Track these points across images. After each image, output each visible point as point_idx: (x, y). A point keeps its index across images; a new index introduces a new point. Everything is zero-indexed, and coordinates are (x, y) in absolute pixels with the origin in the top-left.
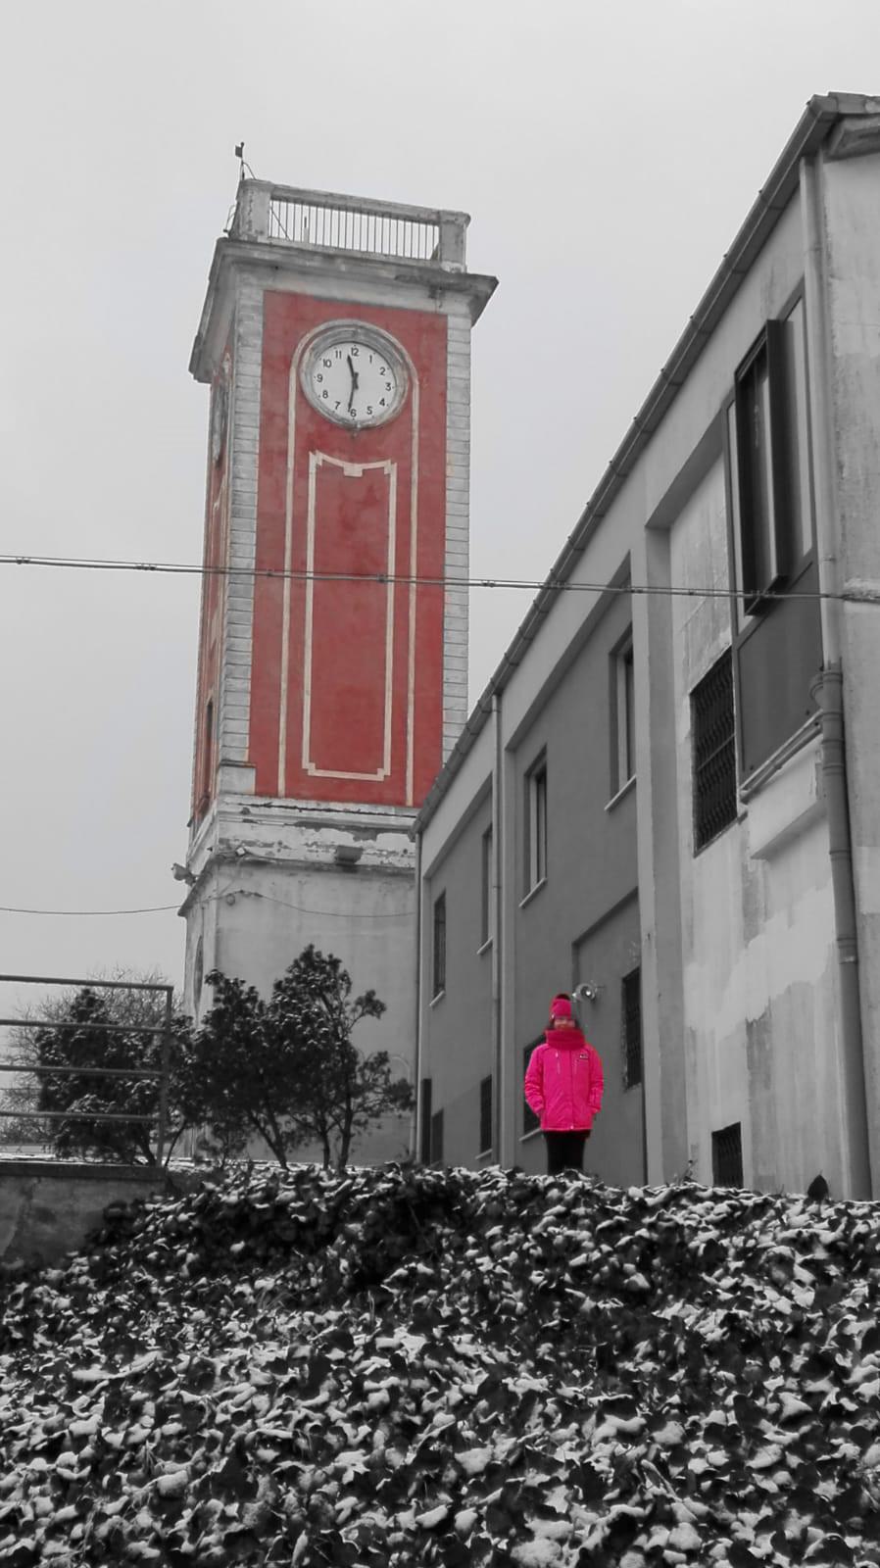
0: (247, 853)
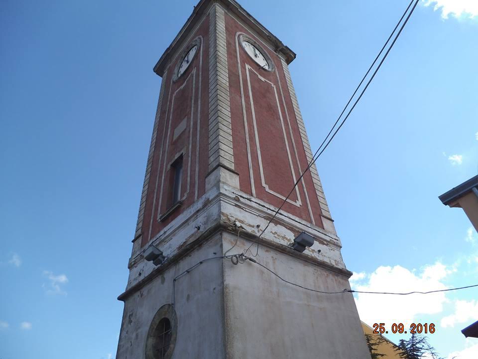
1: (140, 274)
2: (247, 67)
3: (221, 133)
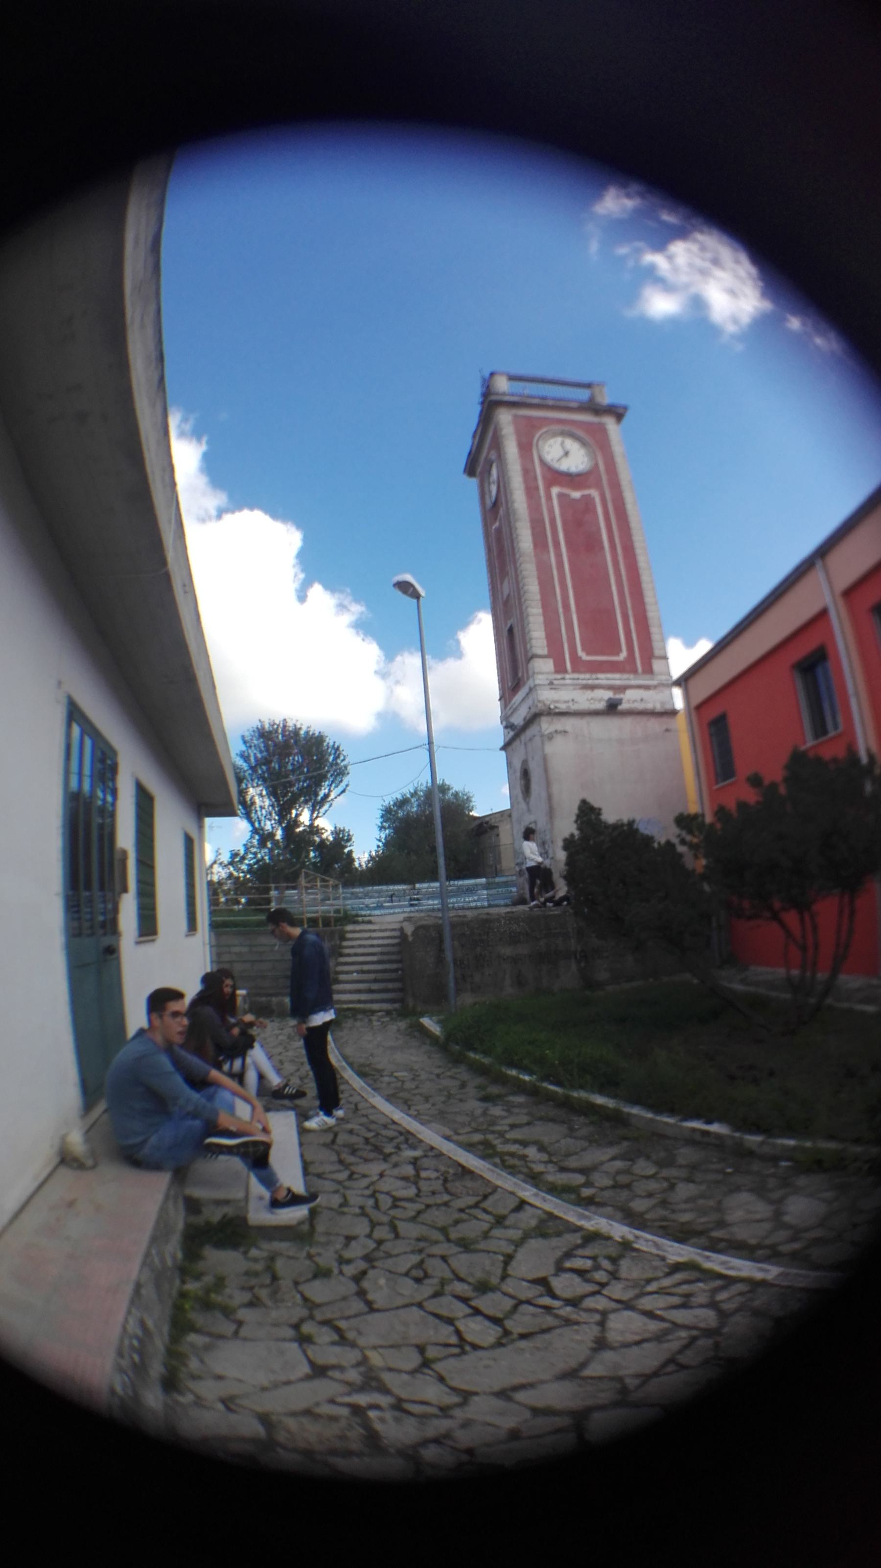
0: (556, 707)
1: (509, 733)
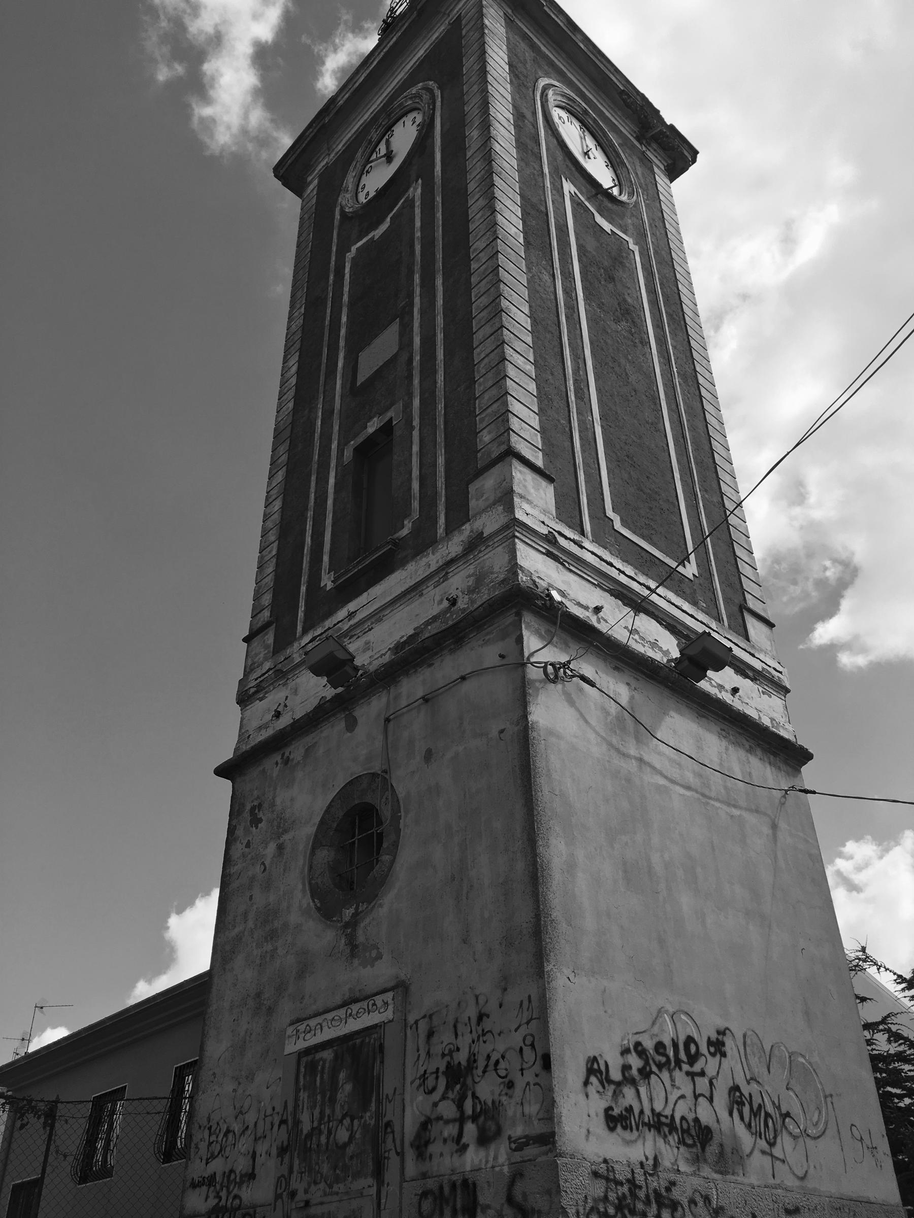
1: (278, 715)
2: (568, 187)
3: (511, 371)
